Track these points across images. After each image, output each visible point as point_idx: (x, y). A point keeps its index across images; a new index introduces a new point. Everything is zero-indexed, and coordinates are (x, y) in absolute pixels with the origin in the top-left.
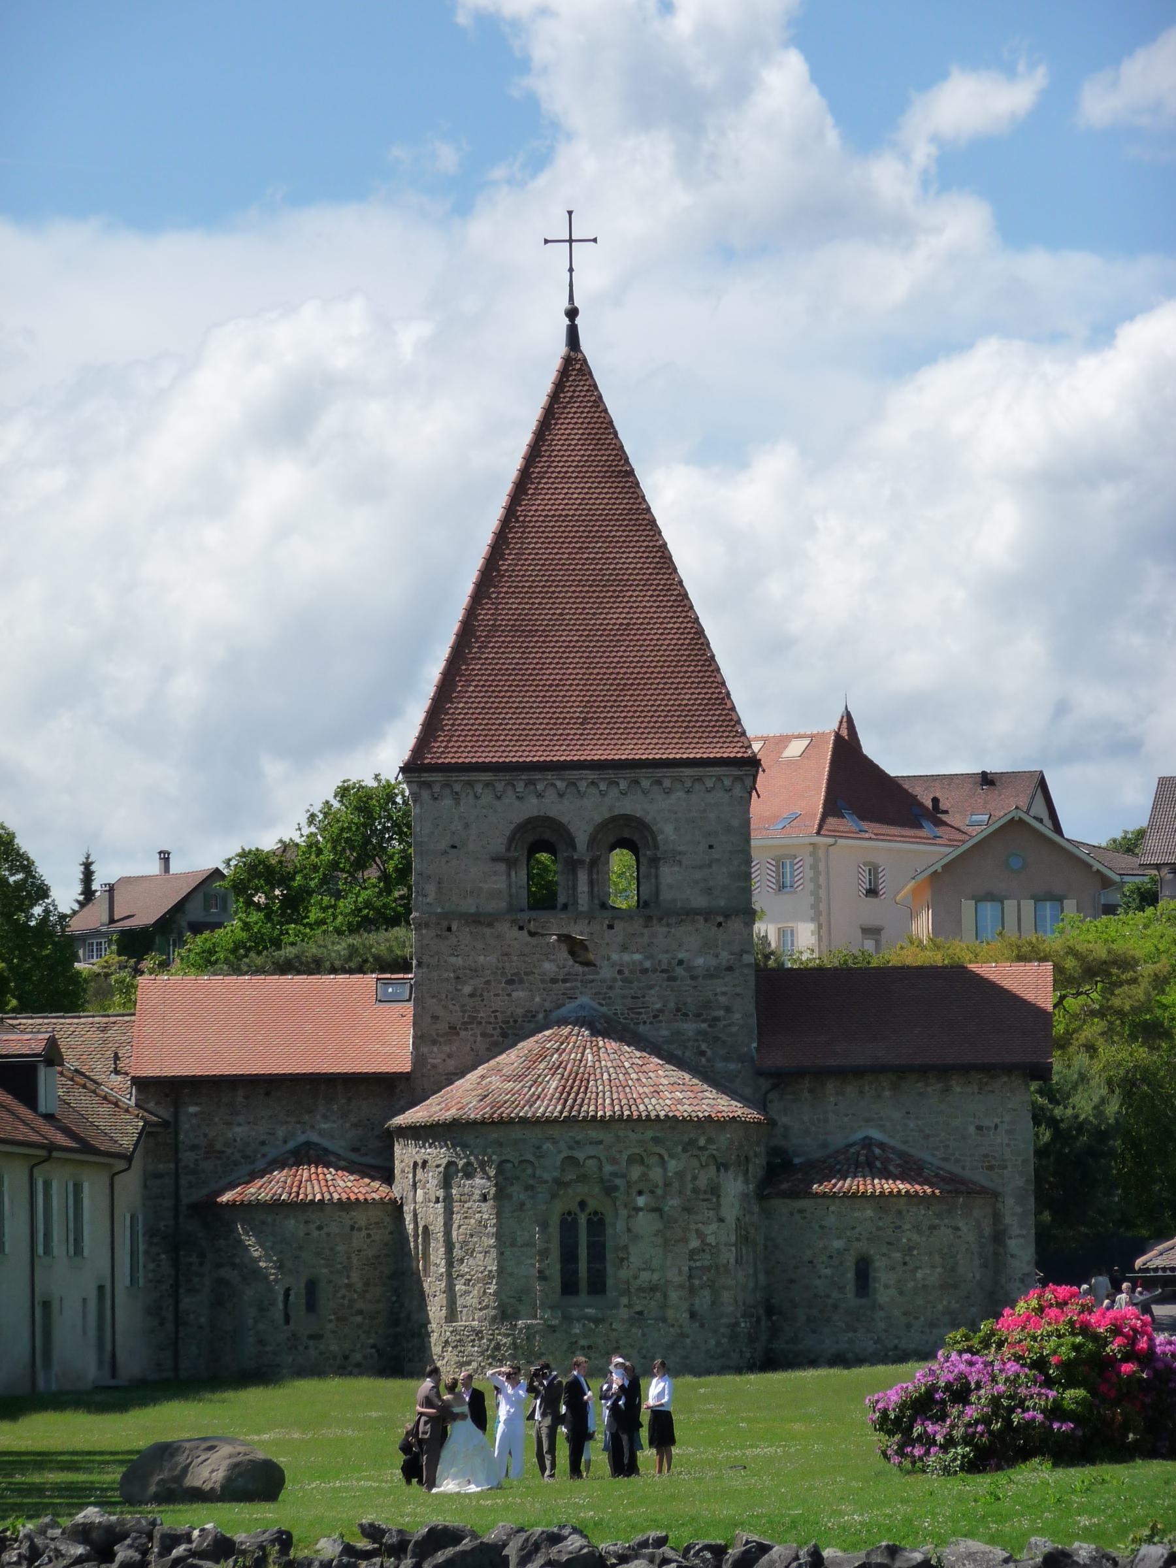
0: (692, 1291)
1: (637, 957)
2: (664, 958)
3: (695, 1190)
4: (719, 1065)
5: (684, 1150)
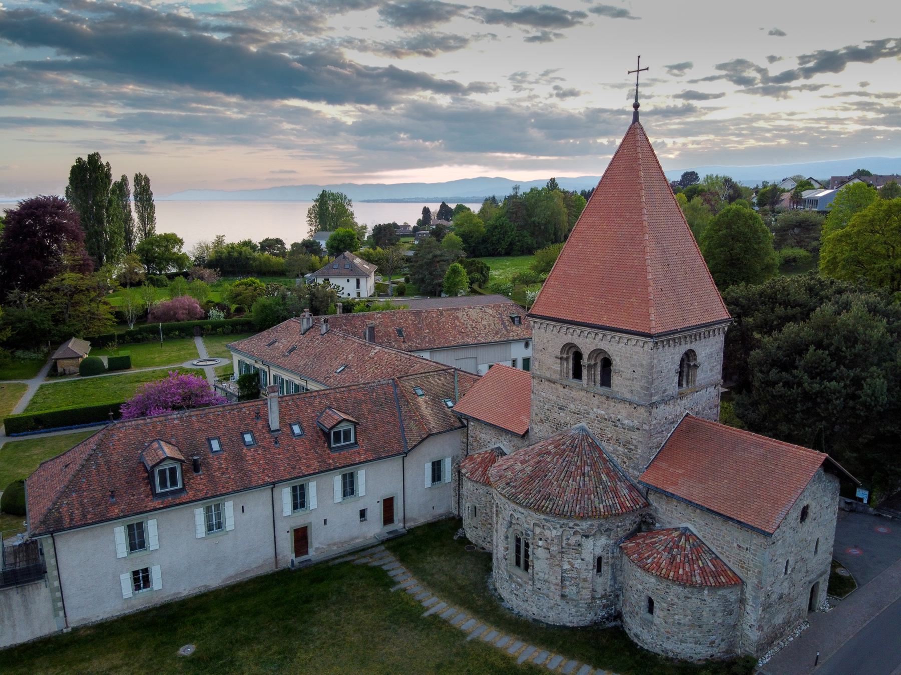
0: (563, 586)
1: (603, 412)
2: (613, 416)
3: (568, 544)
4: (631, 470)
5: (561, 527)
